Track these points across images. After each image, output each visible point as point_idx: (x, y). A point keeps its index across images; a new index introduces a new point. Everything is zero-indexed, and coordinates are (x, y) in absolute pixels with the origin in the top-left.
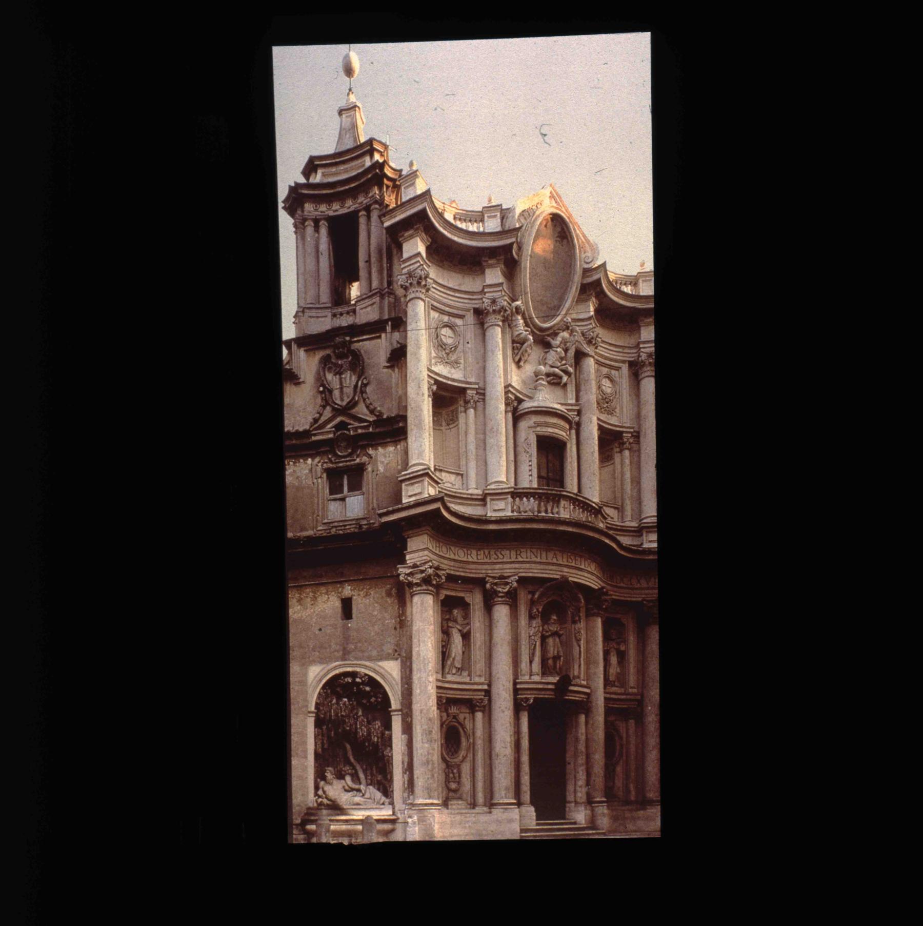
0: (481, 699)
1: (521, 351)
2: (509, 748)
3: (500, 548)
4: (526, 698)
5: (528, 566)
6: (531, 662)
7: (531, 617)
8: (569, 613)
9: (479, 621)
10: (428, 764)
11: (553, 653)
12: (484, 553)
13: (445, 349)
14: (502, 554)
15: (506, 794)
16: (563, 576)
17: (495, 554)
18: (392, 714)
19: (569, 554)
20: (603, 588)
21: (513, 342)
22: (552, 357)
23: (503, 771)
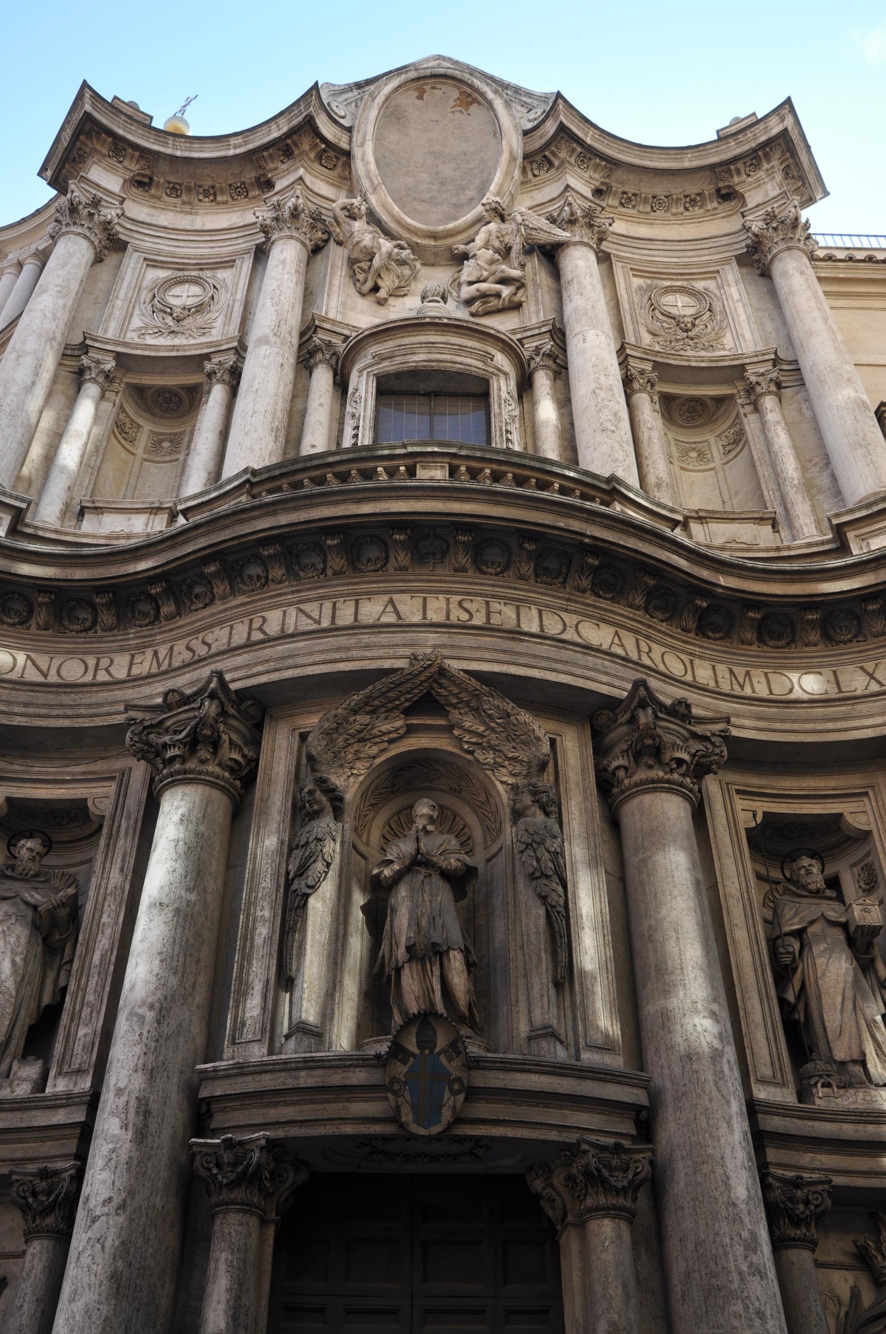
0: (44, 1174)
1: (372, 270)
4: (229, 1144)
5: (282, 649)
8: (500, 787)
9: (122, 870)
12: (156, 654)
13: (171, 314)
14: (204, 643)
16: (414, 658)
17: (188, 648)
19: (456, 599)
20: (639, 684)
21: (352, 262)
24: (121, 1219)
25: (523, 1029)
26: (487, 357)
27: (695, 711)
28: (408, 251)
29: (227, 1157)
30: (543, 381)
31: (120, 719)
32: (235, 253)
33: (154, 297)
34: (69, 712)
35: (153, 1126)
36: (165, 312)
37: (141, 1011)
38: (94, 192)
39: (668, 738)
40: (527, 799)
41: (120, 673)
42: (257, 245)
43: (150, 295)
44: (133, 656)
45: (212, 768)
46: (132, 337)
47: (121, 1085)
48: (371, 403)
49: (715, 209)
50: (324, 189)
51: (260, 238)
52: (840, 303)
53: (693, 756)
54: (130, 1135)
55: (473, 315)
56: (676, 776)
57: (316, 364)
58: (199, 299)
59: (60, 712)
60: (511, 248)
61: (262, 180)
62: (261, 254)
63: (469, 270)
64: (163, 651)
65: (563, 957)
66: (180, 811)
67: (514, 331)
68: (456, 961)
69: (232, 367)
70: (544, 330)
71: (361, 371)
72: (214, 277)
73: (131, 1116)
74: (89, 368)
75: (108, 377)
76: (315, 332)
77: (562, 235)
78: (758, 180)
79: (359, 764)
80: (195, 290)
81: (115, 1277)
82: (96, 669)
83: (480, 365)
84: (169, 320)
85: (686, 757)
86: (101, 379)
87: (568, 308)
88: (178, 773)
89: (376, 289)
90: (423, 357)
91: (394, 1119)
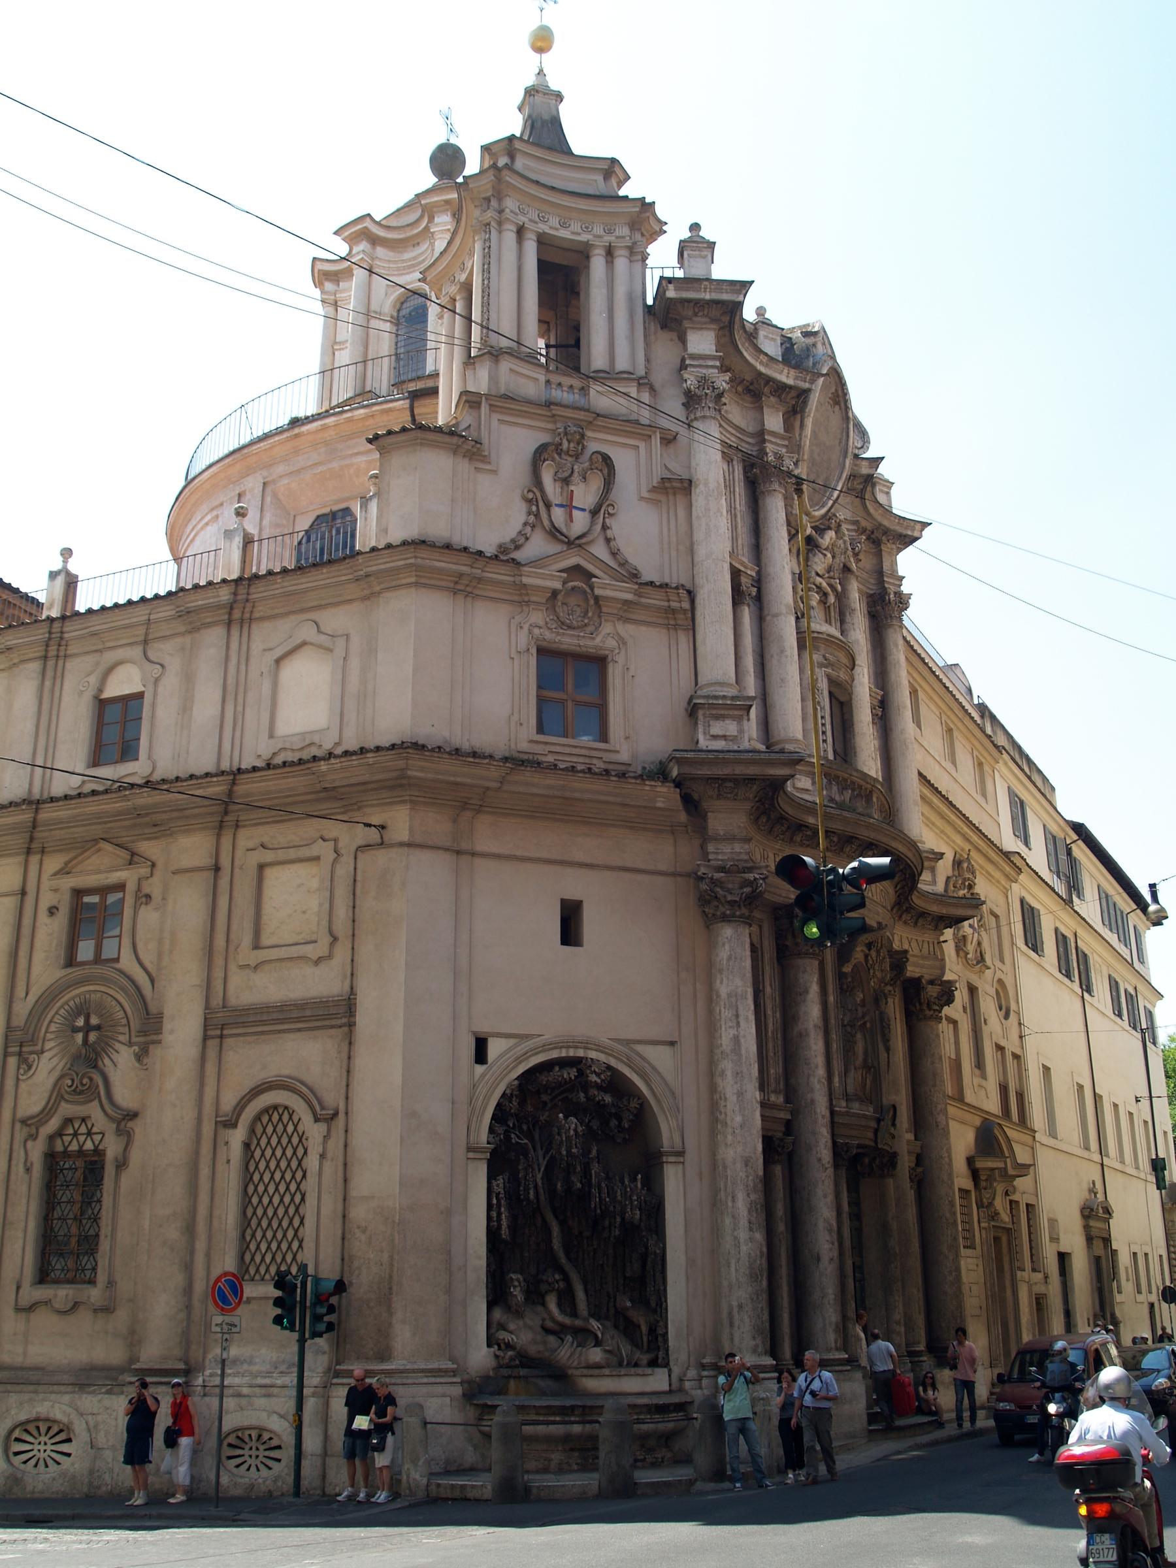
4: (847, 1144)
9: (771, 986)
10: (762, 1276)
11: (865, 1060)
15: (836, 1342)
18: (664, 1159)
22: (820, 563)
23: (830, 1291)
29: (845, 1149)
47: (823, 1113)
61: (751, 387)
77: (854, 566)
78: (892, 549)
91: (876, 1142)
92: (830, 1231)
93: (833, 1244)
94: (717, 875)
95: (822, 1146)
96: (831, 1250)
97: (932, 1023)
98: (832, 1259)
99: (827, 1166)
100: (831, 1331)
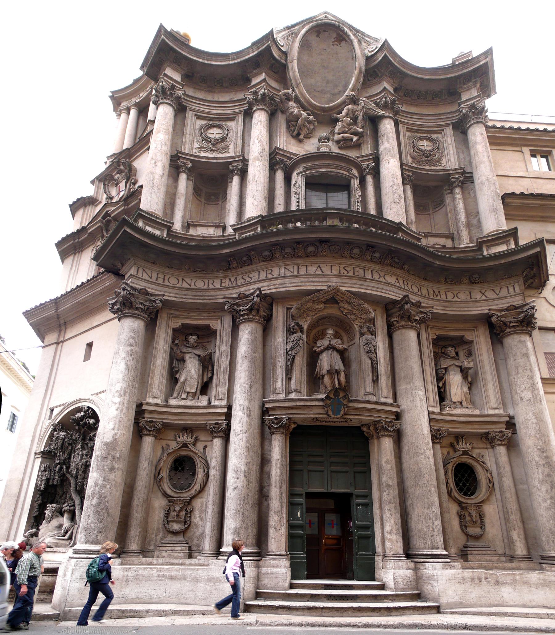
2: (242, 478)
3: (249, 272)
4: (276, 419)
6: (289, 378)
7: (290, 331)
8: (355, 326)
12: (230, 280)
13: (210, 142)
14: (249, 277)
17: (242, 278)
21: (288, 122)
24: (246, 435)
25: (363, 392)
26: (349, 171)
27: (422, 304)
28: (312, 117)
30: (369, 180)
31: (224, 300)
32: (234, 114)
33: (202, 133)
34: (201, 298)
35: (252, 413)
36: (208, 141)
37: (244, 385)
38: (172, 82)
39: (413, 312)
40: (365, 330)
41: (218, 286)
42: (244, 110)
43: (200, 132)
44: (221, 280)
45: (257, 318)
46: (195, 152)
47: (241, 403)
48: (303, 188)
49: (446, 99)
50: (274, 84)
51: (246, 107)
52: (494, 147)
53: (420, 318)
54: (246, 415)
55: (340, 148)
56: (414, 324)
57: (277, 169)
58: (221, 135)
59: (198, 298)
60: (358, 117)
62: (248, 114)
63: (339, 126)
64: (233, 279)
65: (375, 374)
66: (249, 330)
67: (358, 157)
68: (342, 374)
69: (241, 168)
70: (371, 157)
71: (298, 174)
72: (226, 125)
73: (245, 411)
74: (182, 166)
75: (189, 170)
76: (276, 155)
79: (308, 318)
80: (219, 131)
81: (246, 447)
82: (208, 284)
83: (347, 173)
84: (210, 144)
85: (418, 318)
86: (186, 171)
87: (382, 148)
88: (246, 319)
89: (299, 134)
90: (324, 170)
92: (236, 472)
93: (238, 478)
94: (115, 301)
95: (238, 422)
96: (236, 482)
97: (516, 337)
98: (235, 488)
99: (239, 433)
100: (230, 533)
